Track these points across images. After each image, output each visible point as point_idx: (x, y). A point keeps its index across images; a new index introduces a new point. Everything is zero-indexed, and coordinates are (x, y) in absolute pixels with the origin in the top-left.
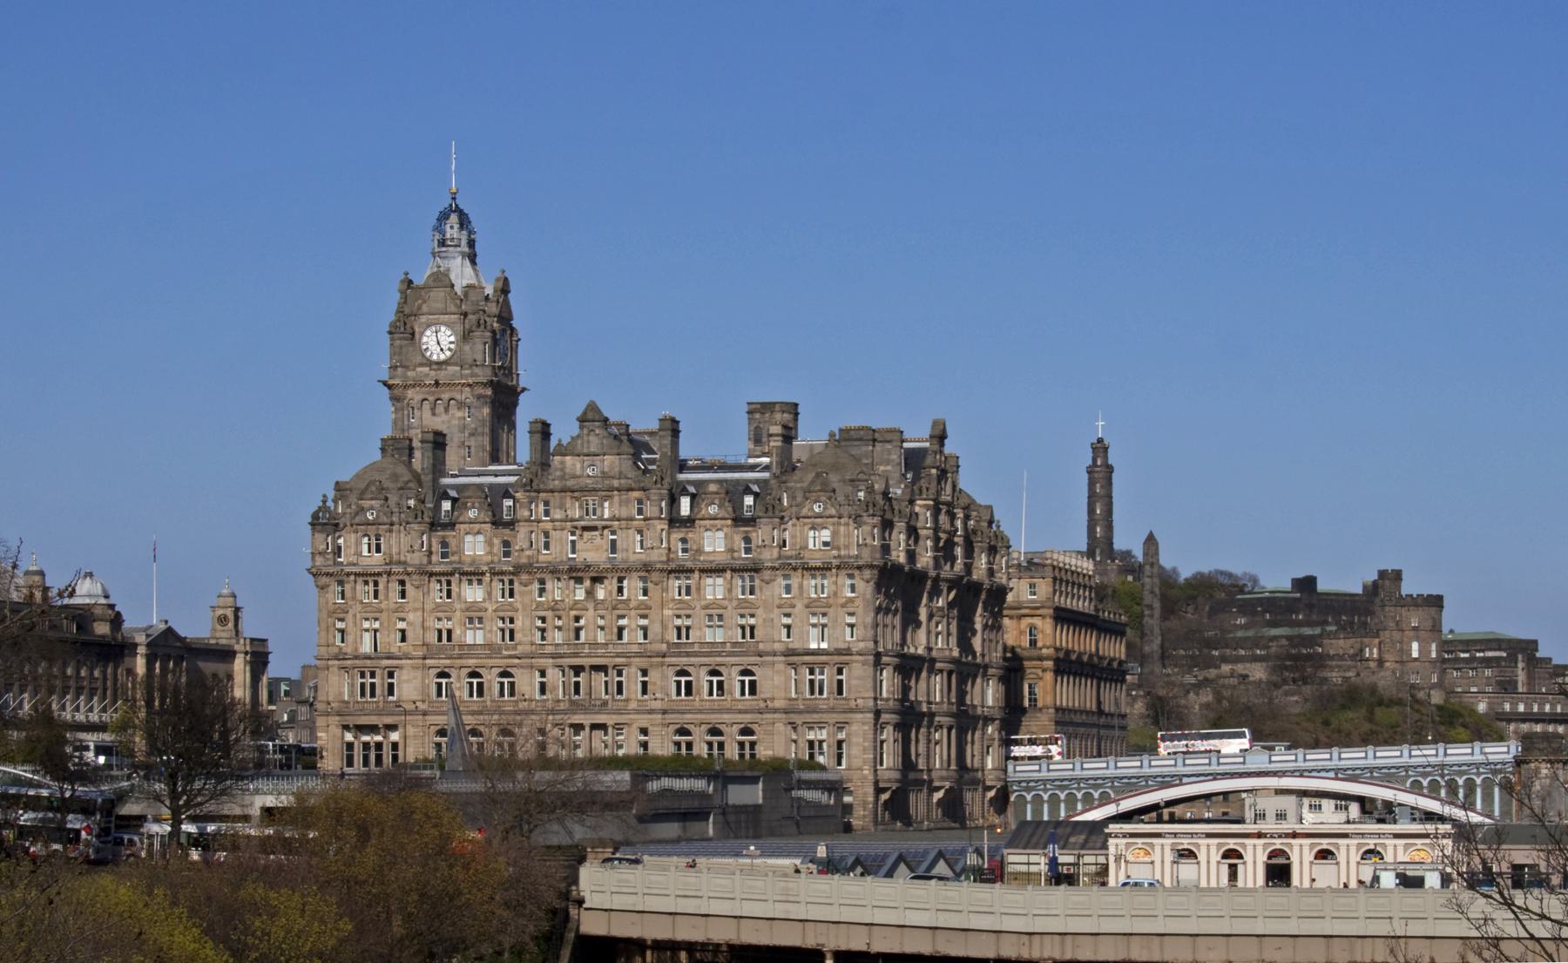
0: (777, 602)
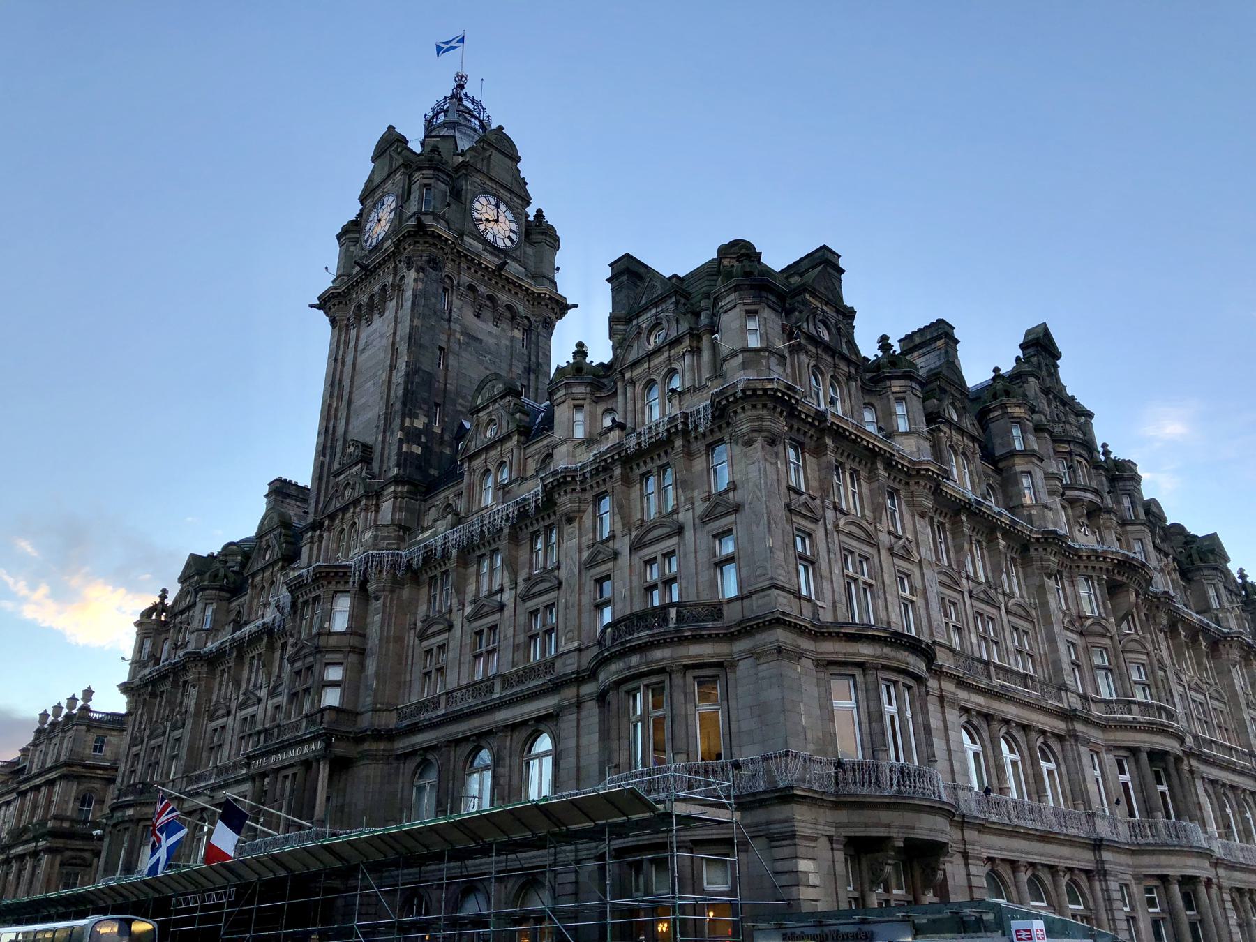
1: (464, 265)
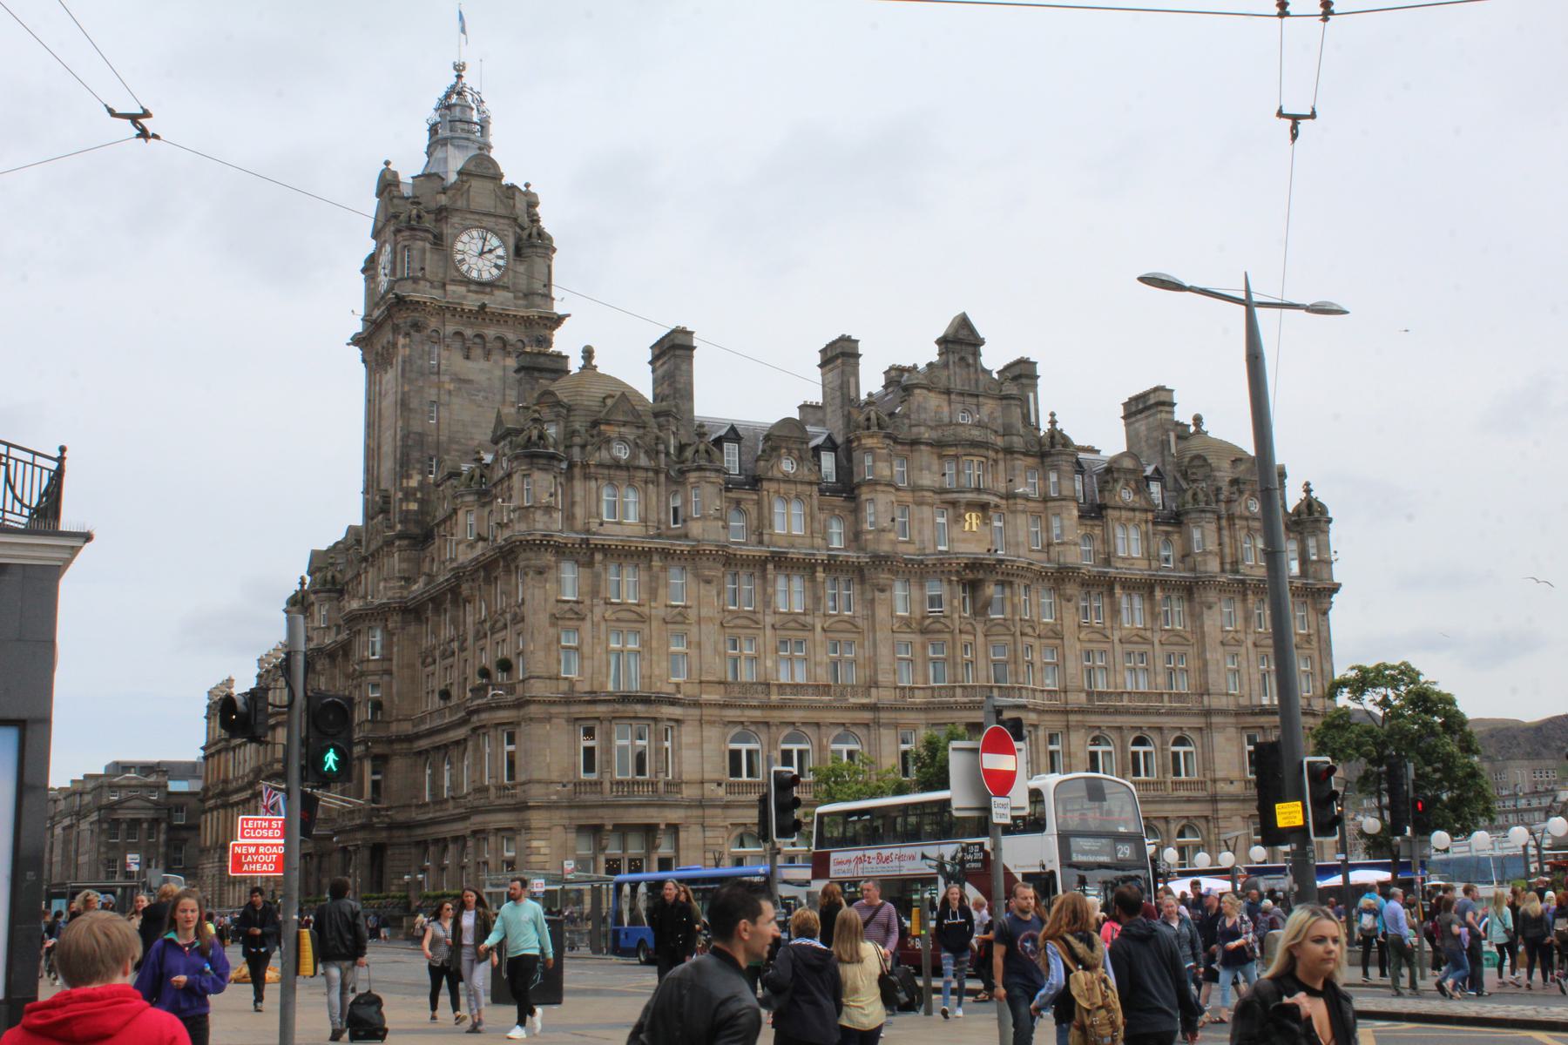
0: (1220, 637)
1: (448, 316)
